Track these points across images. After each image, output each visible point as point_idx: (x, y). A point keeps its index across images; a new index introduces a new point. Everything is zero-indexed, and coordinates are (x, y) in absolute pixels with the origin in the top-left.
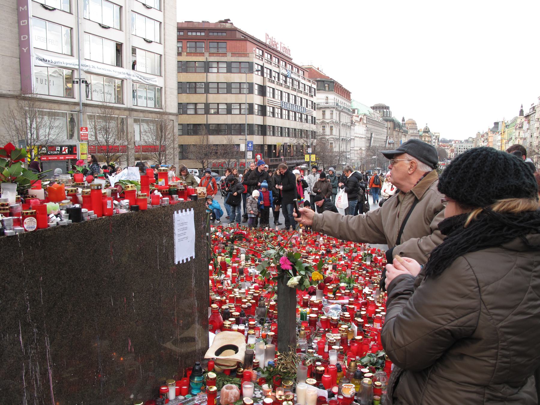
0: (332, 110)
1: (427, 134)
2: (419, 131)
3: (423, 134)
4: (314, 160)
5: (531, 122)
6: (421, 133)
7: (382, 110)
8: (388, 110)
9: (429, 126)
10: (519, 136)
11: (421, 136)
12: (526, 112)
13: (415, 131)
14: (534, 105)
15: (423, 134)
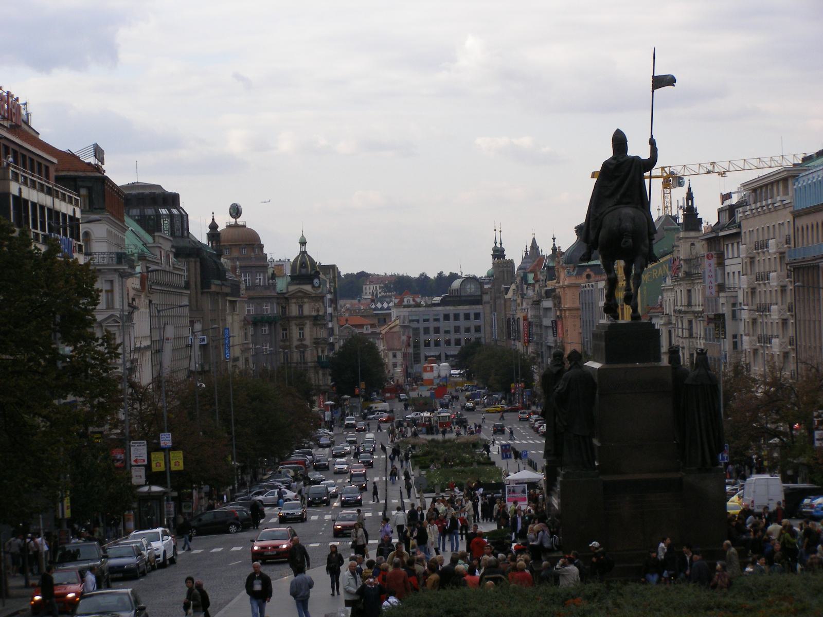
0: (110, 277)
1: (308, 288)
2: (274, 276)
3: (293, 288)
4: (181, 467)
5: (727, 262)
6: (281, 285)
7: (150, 211)
8: (175, 211)
9: (311, 251)
10: (689, 304)
11: (284, 299)
12: (709, 215)
13: (260, 279)
14: (734, 200)
15: (293, 288)
